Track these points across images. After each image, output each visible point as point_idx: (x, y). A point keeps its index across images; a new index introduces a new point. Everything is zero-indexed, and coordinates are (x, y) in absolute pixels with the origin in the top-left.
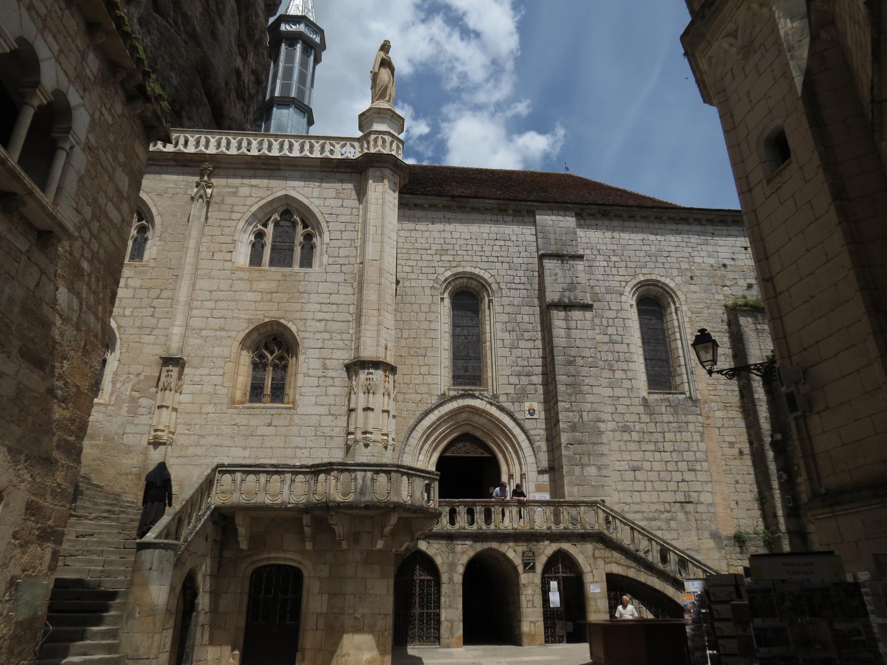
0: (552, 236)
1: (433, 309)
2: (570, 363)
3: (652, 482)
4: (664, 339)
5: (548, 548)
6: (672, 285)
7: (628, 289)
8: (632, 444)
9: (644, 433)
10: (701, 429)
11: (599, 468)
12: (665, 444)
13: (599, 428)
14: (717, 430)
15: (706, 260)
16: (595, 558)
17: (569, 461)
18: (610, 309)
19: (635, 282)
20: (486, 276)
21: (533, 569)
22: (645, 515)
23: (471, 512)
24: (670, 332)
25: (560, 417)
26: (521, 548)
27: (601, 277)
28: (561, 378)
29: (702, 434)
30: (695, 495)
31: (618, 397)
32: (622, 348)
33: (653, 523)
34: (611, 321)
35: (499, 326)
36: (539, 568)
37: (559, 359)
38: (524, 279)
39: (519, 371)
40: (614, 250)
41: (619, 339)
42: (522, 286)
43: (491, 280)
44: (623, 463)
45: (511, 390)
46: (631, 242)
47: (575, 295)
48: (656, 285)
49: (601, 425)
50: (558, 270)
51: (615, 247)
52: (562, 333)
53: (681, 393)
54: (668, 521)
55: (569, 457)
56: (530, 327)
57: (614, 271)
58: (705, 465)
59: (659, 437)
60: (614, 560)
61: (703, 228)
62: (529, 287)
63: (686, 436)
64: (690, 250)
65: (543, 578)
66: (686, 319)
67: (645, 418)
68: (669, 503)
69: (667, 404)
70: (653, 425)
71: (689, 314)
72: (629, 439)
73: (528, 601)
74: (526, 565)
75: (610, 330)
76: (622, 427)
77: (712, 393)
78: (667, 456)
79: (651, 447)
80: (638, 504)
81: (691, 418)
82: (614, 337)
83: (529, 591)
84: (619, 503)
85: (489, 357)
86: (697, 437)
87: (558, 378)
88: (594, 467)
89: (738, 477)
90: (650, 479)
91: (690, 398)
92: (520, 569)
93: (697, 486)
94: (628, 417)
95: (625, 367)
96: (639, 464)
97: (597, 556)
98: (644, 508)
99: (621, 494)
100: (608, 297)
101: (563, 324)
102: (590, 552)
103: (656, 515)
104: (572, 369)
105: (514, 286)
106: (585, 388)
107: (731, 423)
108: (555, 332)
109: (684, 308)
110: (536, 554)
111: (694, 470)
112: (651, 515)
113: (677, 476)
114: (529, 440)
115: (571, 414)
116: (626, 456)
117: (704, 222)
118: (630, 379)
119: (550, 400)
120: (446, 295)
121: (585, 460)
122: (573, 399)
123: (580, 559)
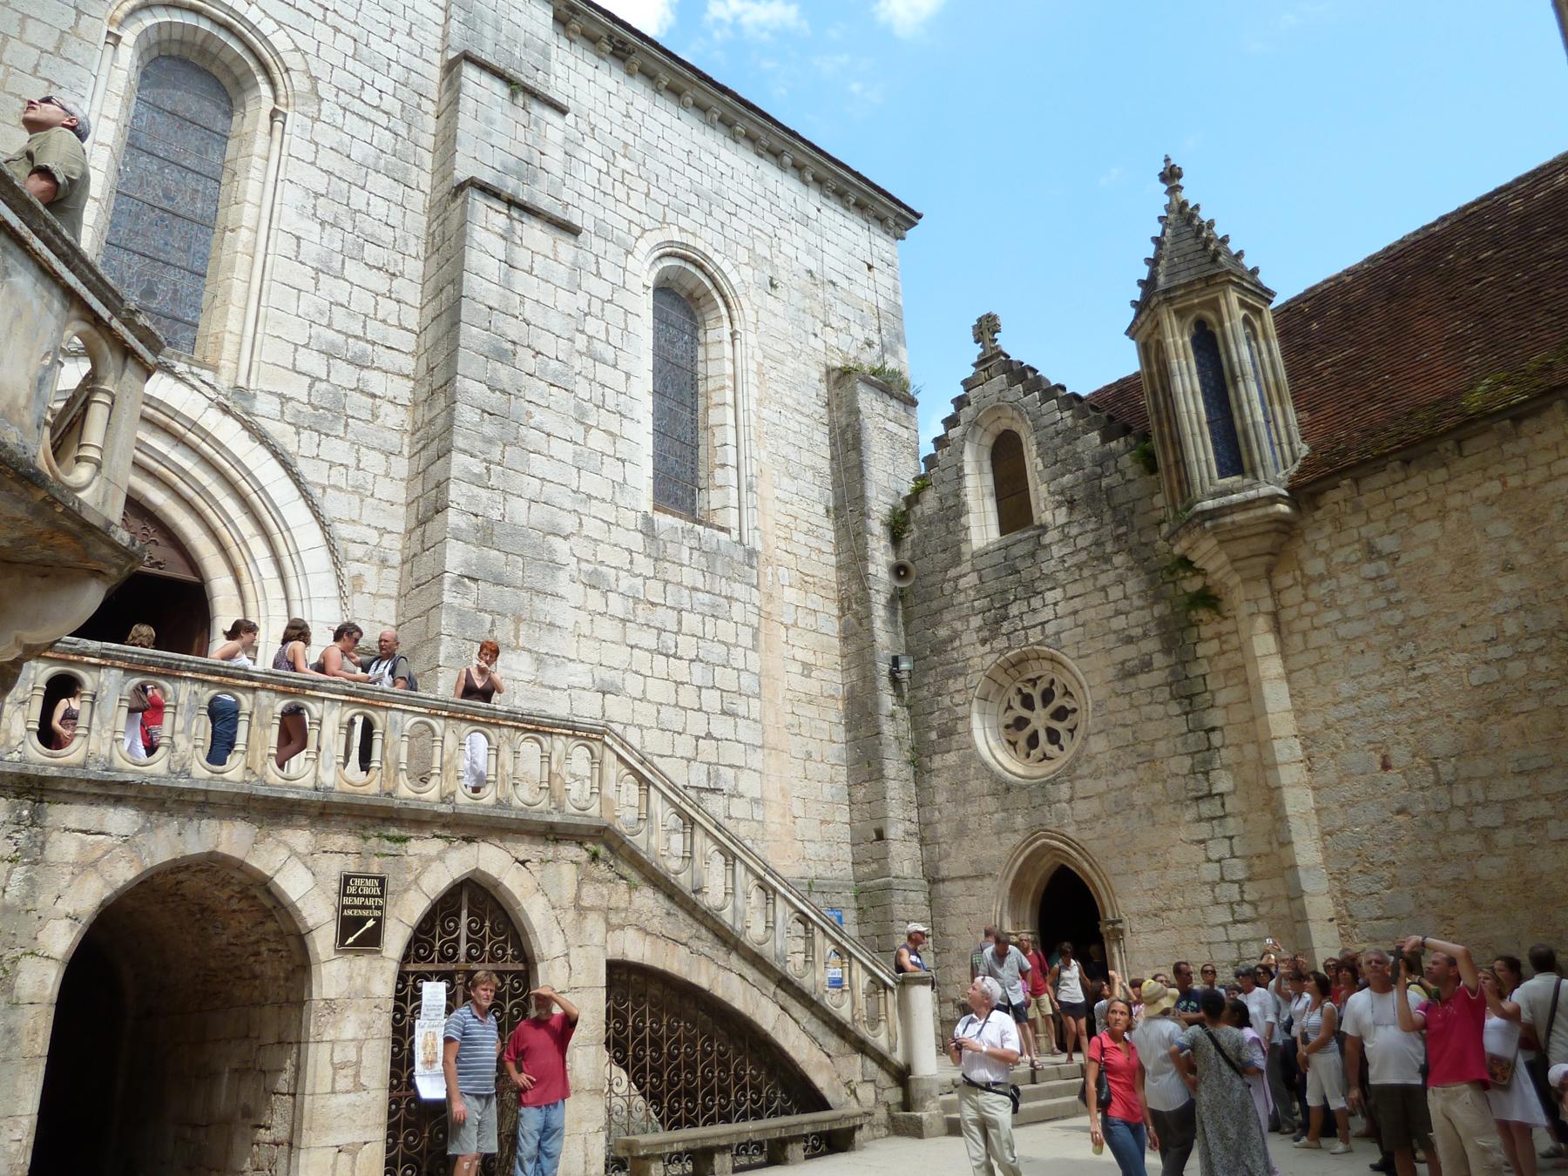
0: (488, 32)
1: (72, 48)
2: (501, 356)
3: (640, 727)
4: (695, 395)
5: (436, 866)
6: (734, 278)
7: (644, 246)
9: (637, 600)
10: (754, 620)
11: (540, 660)
12: (680, 638)
13: (551, 551)
14: (783, 630)
15: (802, 256)
16: (581, 910)
17: (460, 625)
18: (598, 275)
19: (660, 237)
20: (280, 41)
21: (373, 941)
23: (147, 711)
24: (711, 385)
25: (455, 492)
26: (341, 852)
27: (588, 191)
28: (470, 387)
29: (756, 632)
30: (730, 773)
31: (589, 496)
32: (614, 378)
34: (596, 307)
35: (291, 195)
36: (395, 939)
37: (471, 334)
38: (389, 103)
39: (333, 344)
40: (626, 144)
41: (609, 354)
42: (383, 120)
43: (293, 60)
44: (580, 667)
45: (297, 388)
46: (662, 144)
47: (531, 194)
48: (701, 267)
49: (557, 543)
50: (496, 113)
51: (630, 139)
52: (492, 268)
53: (722, 529)
55: (461, 614)
56: (387, 235)
57: (620, 192)
58: (754, 702)
59: (668, 618)
60: (632, 919)
61: (804, 189)
62: (403, 131)
63: (725, 630)
64: (776, 222)
65: (402, 977)
66: (753, 366)
67: (644, 565)
69: (694, 543)
70: (660, 585)
71: (759, 357)
73: (336, 1068)
74: (347, 925)
75: (592, 326)
77: (782, 545)
78: (680, 669)
79: (649, 639)
81: (739, 590)
82: (599, 347)
83: (349, 1027)
85: (240, 272)
86: (746, 638)
87: (462, 384)
88: (526, 657)
89: (812, 746)
90: (639, 720)
91: (740, 542)
92: (323, 940)
93: (734, 754)
94: (605, 552)
95: (615, 429)
96: (615, 677)
97: (585, 903)
100: (598, 245)
101: (498, 247)
102: (569, 892)
104: (504, 373)
105: (357, 106)
106: (533, 437)
107: (811, 619)
108: (473, 258)
109: (751, 339)
110: (391, 886)
111: (734, 715)
113: (697, 724)
114: (333, 551)
115: (484, 493)
116: (588, 651)
117: (810, 178)
118: (623, 461)
119: (434, 441)
120: (129, 36)
123: (536, 913)
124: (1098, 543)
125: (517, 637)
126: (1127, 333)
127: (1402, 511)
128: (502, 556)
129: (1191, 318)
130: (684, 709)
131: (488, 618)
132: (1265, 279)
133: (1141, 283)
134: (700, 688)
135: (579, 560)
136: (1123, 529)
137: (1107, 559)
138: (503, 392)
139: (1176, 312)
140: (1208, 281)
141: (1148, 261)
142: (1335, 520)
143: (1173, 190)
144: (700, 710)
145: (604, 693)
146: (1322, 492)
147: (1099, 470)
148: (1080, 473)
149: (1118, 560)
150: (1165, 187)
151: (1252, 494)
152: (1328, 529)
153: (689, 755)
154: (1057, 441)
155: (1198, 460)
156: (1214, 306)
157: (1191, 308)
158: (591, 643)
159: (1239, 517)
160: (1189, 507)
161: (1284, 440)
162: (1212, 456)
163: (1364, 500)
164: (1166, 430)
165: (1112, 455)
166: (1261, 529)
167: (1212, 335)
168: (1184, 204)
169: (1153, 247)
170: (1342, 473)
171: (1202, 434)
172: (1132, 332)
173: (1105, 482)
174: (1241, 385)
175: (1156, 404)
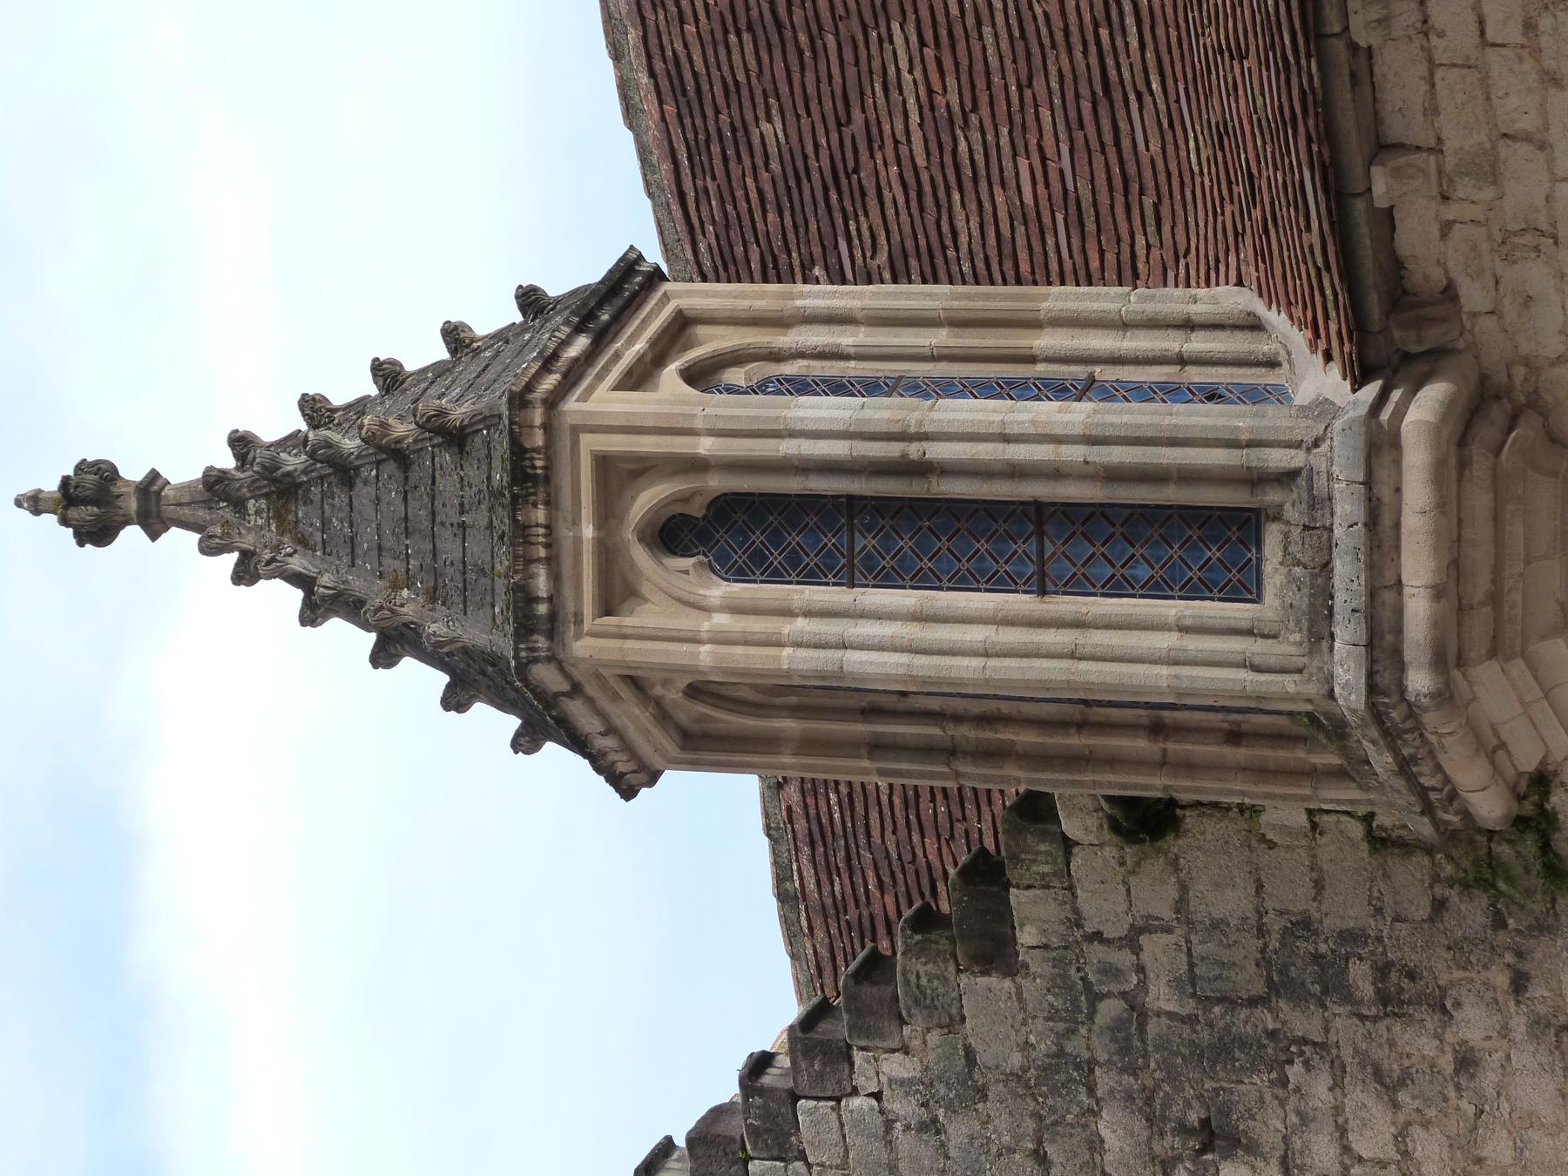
124: (1389, 1085)
126: (628, 793)
127: (1529, 26)
129: (640, 556)
132: (573, 270)
133: (455, 700)
136: (1360, 977)
137: (1466, 1062)
139: (607, 607)
140: (529, 477)
141: (383, 657)
142: (1506, 248)
143: (154, 507)
146: (1396, 266)
147: (1110, 1009)
148: (1105, 1080)
149: (1473, 1023)
150: (132, 535)
151: (1347, 508)
152: (1535, 275)
154: (958, 1131)
155: (1174, 660)
156: (617, 476)
157: (608, 554)
159: (1417, 567)
160: (1335, 730)
161: (1171, 343)
162: (1172, 609)
163: (1460, 138)
164: (1027, 738)
165: (1063, 954)
166: (1480, 501)
167: (727, 508)
168: (214, 482)
169: (337, 628)
170: (1339, 193)
171: (1079, 624)
172: (628, 780)
173: (1161, 997)
174: (938, 451)
175: (926, 751)
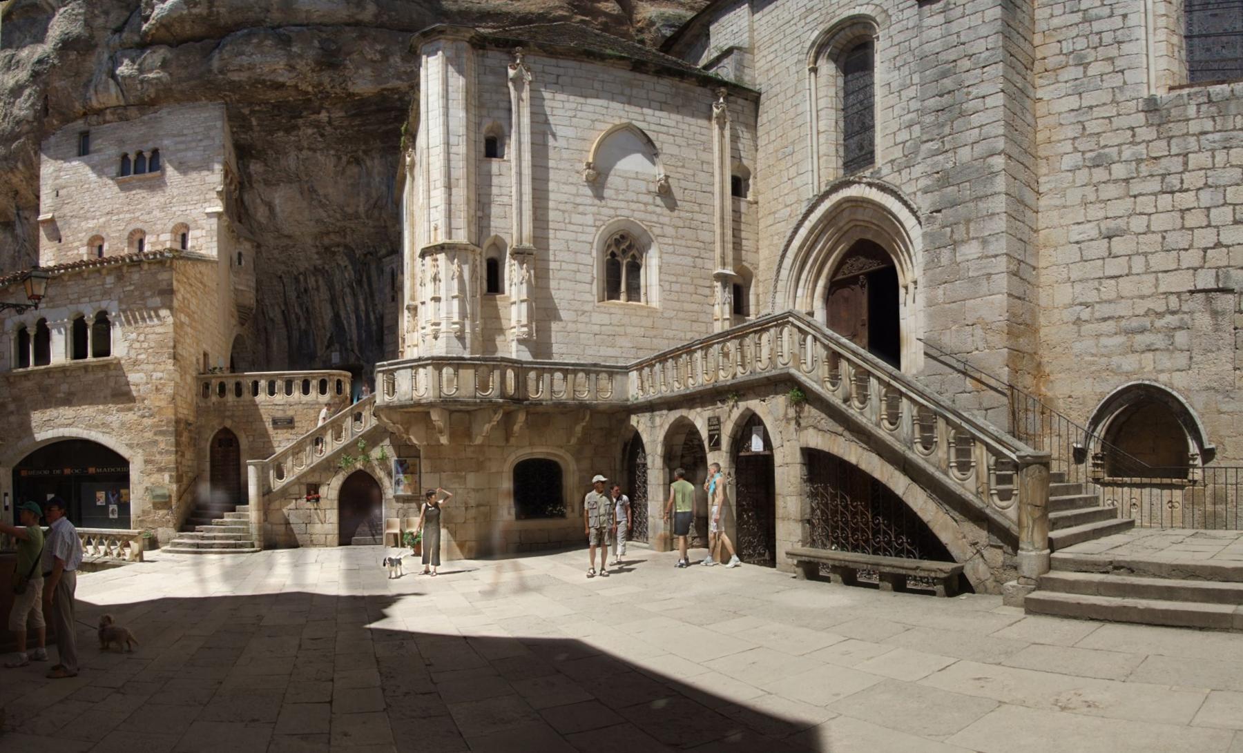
3: (1145, 254)
8: (1111, 186)
11: (984, 242)
22: (1123, 323)
33: (1139, 338)
54: (1171, 331)
68: (1179, 294)
72: (1106, 177)
76: (1094, 159)
78: (1187, 199)
79: (1155, 185)
80: (1110, 302)
84: (1071, 305)
90: (1144, 248)
96: (1121, 223)
98: (1122, 309)
99: (1078, 287)
103: (1146, 322)
104: (948, 83)
112: (1135, 323)
113: (1208, 237)
116: (1095, 212)
121: (960, 233)
122: (947, 130)
125: (968, 233)
128: (956, 188)
130: (1191, 229)
131: (949, 229)
134: (1208, 209)
135: (1083, 153)
138: (949, 92)
144: (1209, 226)
145: (1110, 238)
153: (1196, 265)
158: (1098, 205)
